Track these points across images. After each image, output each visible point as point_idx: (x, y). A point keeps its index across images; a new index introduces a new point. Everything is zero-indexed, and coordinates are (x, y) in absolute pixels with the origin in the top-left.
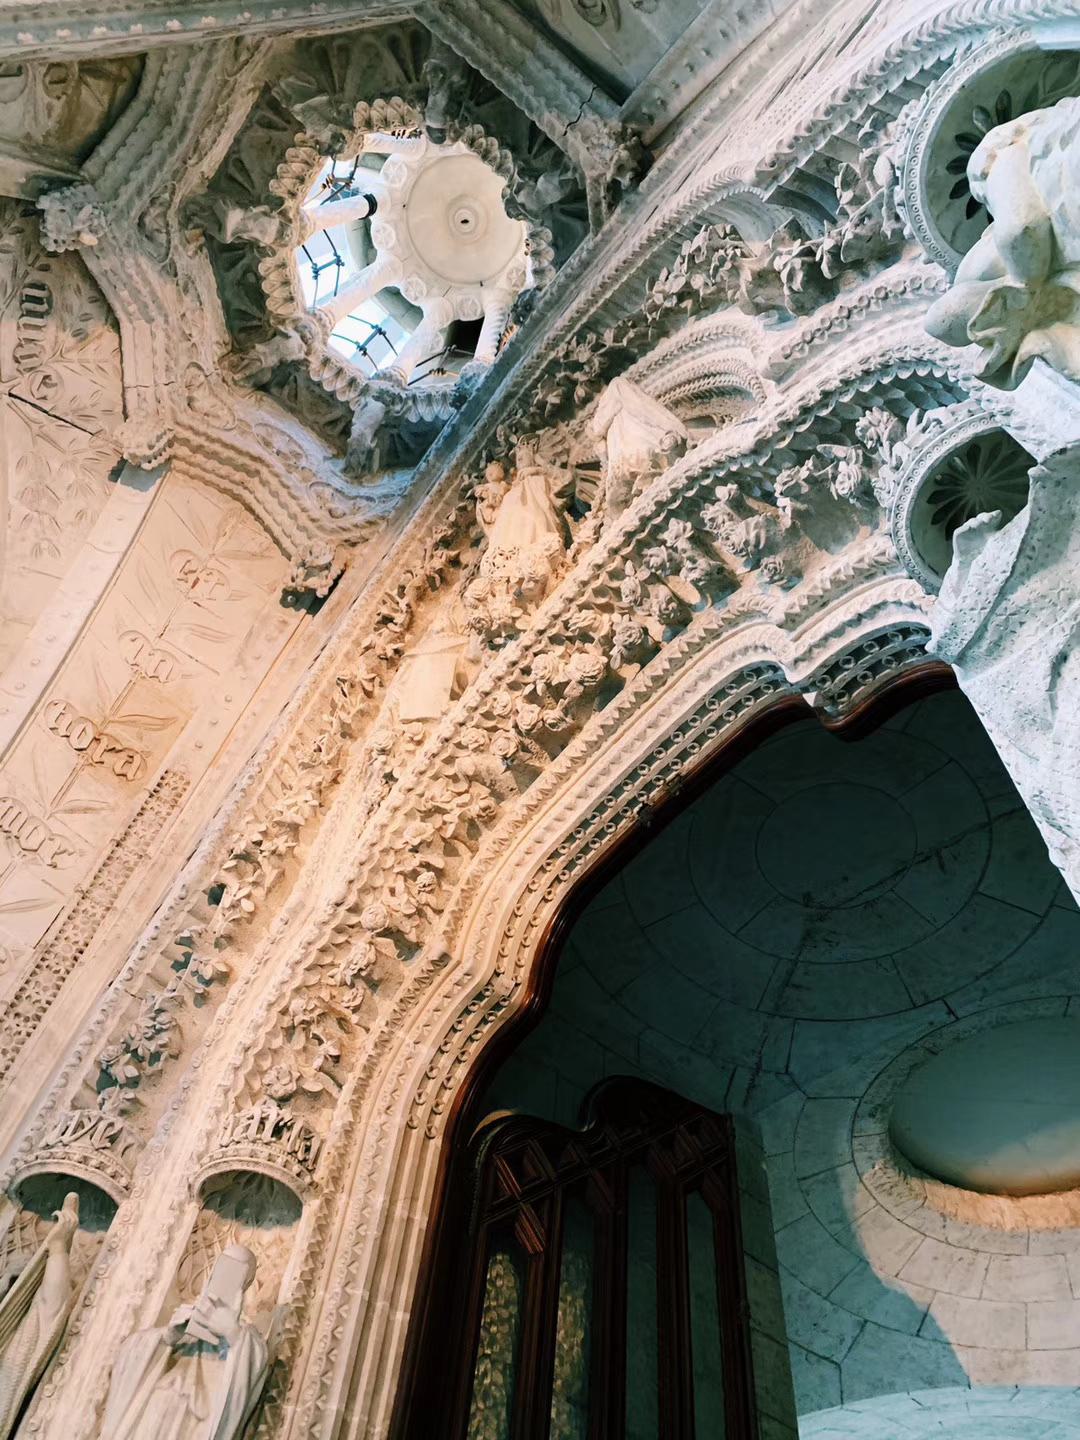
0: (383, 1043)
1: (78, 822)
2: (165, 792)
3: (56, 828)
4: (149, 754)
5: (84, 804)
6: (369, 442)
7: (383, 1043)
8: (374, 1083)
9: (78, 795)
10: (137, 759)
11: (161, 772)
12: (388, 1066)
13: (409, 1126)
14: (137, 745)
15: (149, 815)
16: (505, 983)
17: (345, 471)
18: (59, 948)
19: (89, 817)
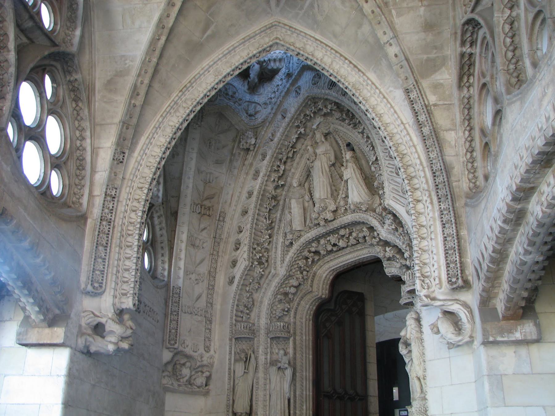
0: (299, 304)
1: (204, 233)
2: (221, 219)
3: (200, 237)
4: (213, 206)
5: (203, 228)
6: (256, 80)
7: (299, 304)
8: (298, 312)
9: (202, 226)
10: (211, 209)
11: (219, 213)
12: (300, 308)
13: (306, 320)
14: (210, 205)
15: (219, 226)
16: (324, 296)
17: (249, 89)
18: (212, 270)
19: (205, 231)
